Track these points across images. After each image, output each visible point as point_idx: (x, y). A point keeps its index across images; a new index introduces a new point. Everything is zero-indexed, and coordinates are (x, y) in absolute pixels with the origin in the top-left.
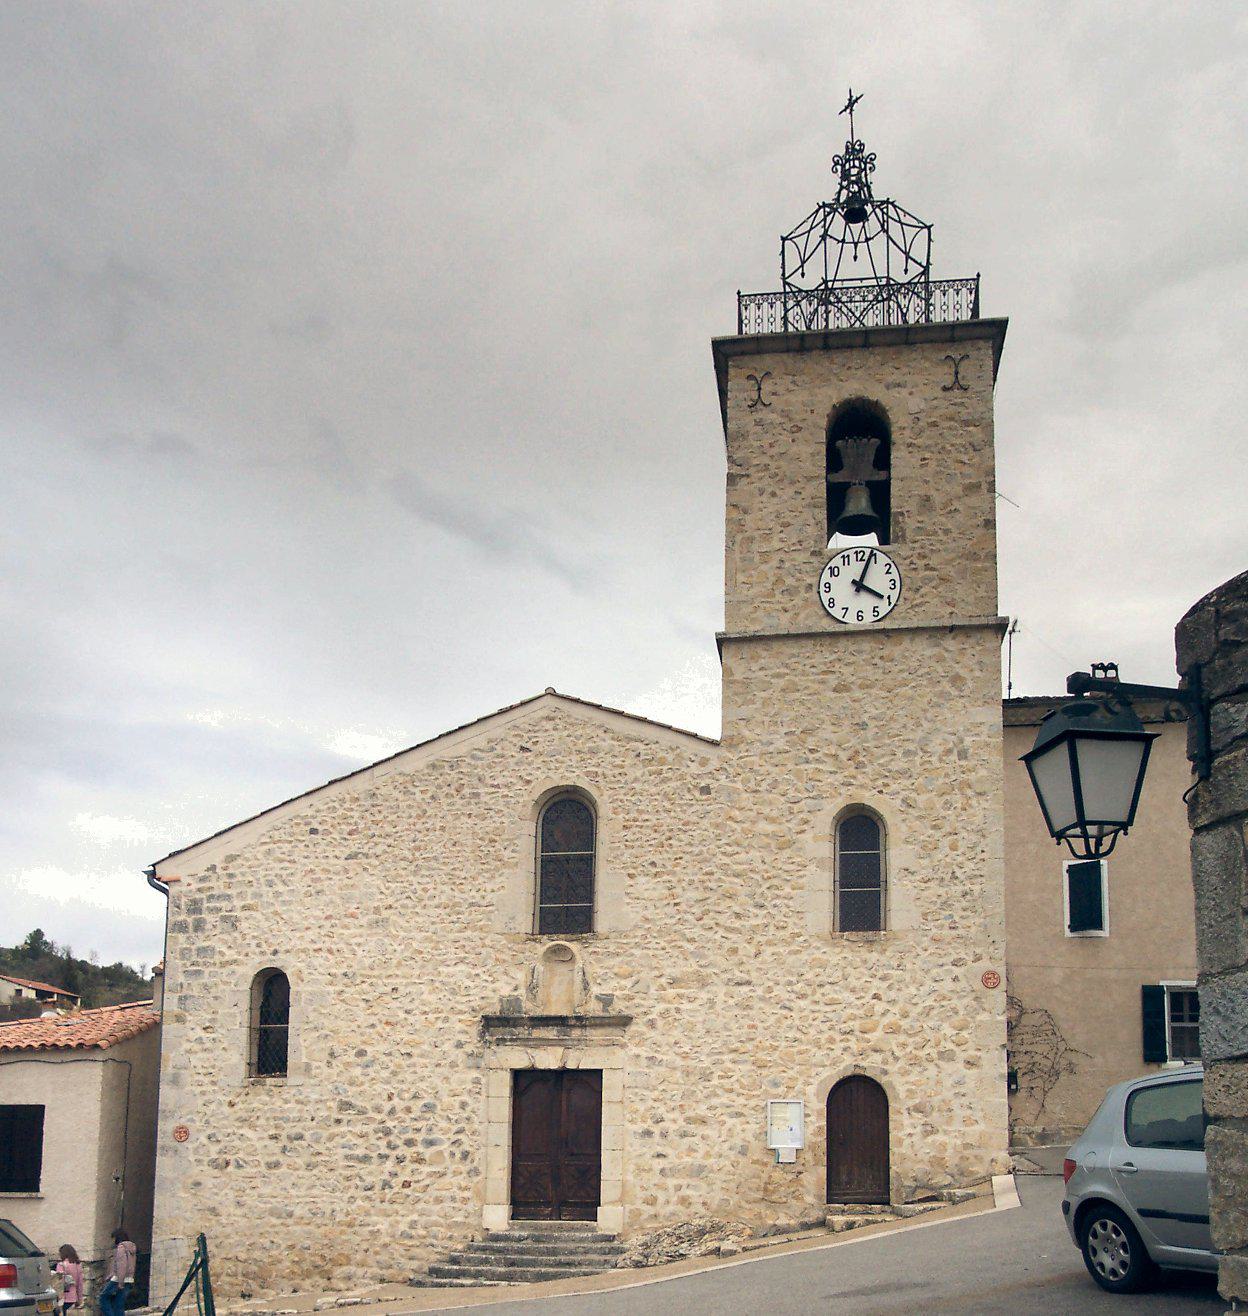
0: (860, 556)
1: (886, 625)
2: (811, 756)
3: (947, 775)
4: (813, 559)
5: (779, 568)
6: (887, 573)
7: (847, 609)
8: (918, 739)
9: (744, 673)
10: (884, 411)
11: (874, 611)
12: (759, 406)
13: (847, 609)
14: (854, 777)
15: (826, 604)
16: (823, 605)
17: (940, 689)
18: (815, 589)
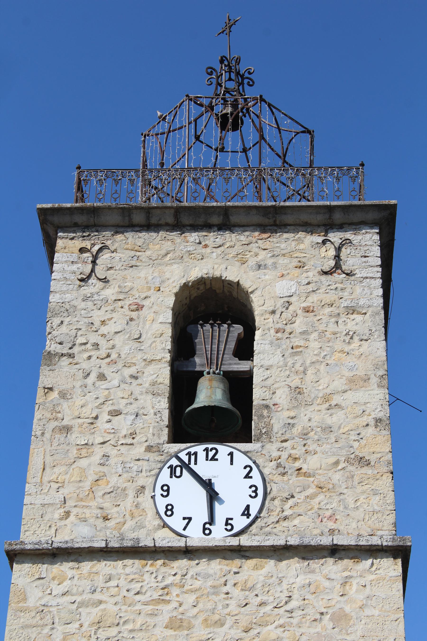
0: (211, 454)
6: (247, 476)
7: (190, 519)
9: (40, 598)
10: (247, 294)
11: (227, 524)
12: (93, 280)
13: (190, 519)
16: (158, 513)
17: (319, 629)
18: (148, 493)
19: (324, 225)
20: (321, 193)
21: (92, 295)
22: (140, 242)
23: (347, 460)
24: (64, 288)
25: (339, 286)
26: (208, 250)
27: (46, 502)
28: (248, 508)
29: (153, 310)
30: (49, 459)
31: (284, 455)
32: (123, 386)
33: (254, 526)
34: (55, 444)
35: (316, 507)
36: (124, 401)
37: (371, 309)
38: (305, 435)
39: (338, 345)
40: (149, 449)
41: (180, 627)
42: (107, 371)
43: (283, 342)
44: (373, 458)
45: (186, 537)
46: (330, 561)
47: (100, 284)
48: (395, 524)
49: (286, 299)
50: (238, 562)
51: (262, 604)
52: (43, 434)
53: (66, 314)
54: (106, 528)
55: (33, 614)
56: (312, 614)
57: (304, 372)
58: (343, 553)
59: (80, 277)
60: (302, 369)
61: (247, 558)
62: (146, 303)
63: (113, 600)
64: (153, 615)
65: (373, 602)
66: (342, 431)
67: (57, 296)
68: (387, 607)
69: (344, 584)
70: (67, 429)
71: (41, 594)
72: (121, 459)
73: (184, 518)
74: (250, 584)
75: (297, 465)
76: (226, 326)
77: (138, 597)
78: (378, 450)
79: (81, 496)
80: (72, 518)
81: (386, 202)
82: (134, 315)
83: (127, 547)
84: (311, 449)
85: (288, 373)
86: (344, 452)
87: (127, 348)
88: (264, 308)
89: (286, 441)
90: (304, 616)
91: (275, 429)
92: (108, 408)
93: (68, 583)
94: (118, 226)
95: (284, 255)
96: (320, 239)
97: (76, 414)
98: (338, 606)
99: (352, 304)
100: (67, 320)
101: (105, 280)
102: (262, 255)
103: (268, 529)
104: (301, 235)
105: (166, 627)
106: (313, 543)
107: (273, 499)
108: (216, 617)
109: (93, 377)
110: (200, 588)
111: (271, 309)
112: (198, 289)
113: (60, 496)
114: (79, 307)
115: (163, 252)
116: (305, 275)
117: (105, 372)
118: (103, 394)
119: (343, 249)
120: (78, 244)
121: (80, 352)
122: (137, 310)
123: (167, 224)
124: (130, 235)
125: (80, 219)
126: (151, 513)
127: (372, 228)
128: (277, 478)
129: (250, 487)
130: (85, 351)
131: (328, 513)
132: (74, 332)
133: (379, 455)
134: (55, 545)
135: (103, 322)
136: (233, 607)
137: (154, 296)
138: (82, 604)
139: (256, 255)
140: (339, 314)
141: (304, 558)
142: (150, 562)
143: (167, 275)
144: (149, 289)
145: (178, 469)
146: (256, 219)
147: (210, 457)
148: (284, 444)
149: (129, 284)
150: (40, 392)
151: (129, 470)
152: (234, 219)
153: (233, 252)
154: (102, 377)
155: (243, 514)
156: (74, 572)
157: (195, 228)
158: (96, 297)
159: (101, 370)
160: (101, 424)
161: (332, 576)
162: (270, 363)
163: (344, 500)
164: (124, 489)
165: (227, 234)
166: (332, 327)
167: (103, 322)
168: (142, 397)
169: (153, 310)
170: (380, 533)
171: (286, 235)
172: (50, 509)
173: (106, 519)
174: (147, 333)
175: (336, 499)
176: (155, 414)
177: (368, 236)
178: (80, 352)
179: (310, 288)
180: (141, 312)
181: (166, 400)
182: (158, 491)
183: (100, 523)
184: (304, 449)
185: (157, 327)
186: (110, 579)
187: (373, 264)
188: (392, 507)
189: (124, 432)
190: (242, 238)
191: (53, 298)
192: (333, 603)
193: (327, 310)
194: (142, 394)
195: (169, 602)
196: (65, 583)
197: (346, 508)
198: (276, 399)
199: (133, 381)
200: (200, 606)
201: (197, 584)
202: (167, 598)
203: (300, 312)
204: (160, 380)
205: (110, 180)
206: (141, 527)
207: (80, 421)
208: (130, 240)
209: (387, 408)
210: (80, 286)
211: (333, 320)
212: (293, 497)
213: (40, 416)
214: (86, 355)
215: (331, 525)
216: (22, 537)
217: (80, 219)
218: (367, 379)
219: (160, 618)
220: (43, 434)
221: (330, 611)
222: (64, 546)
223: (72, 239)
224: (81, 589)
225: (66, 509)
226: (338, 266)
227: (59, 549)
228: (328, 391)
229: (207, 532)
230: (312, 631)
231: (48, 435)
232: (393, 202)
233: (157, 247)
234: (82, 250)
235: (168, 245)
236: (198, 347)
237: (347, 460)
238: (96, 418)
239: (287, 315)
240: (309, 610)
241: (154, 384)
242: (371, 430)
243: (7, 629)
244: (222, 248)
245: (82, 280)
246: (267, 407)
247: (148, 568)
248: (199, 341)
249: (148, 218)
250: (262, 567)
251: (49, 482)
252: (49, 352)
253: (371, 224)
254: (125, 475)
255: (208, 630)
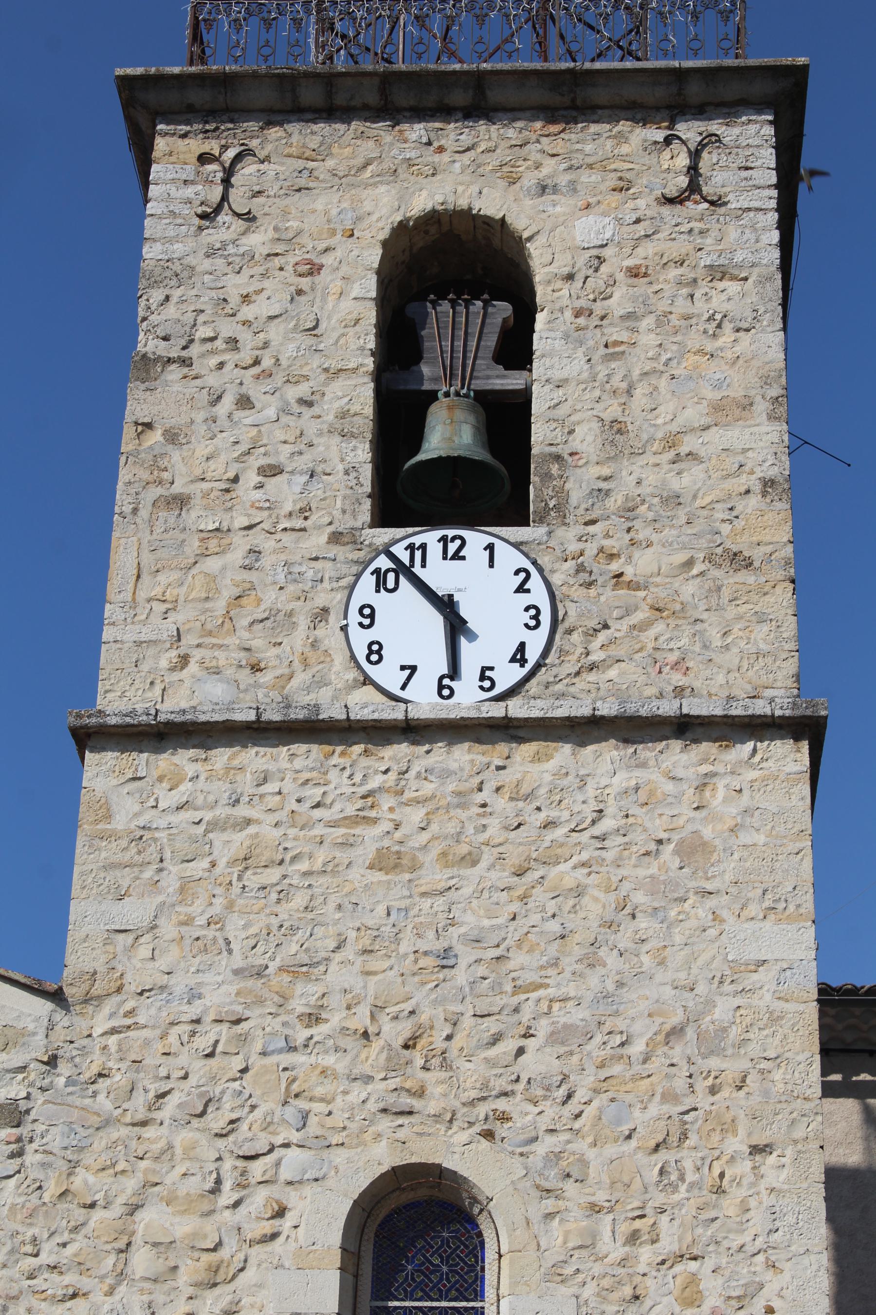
0: (452, 547)
1: (517, 708)
2: (301, 1035)
3: (669, 1097)
4: (335, 550)
5: (247, 568)
6: (521, 589)
7: (413, 669)
8: (590, 996)
9: (136, 815)
11: (482, 678)
12: (224, 217)
13: (413, 669)
14: (420, 1093)
15: (361, 654)
16: (353, 657)
17: (653, 870)
18: (335, 621)
19: (669, 107)
20: (663, 45)
21: (224, 247)
22: (313, 142)
23: (709, 558)
24: (171, 233)
25: (697, 225)
26: (446, 157)
27: (143, 637)
28: (522, 647)
29: (341, 274)
30: (147, 559)
31: (591, 549)
32: (284, 419)
33: (534, 682)
34: (158, 529)
35: (650, 645)
36: (288, 449)
37: (756, 271)
38: (629, 511)
39: (694, 340)
40: (336, 538)
41: (396, 866)
42: (255, 391)
43: (589, 334)
44: (757, 554)
45: (406, 702)
46: (676, 745)
47: (239, 225)
48: (798, 677)
49: (595, 252)
50: (503, 748)
51: (549, 825)
52: (135, 511)
53: (174, 282)
54: (257, 685)
55: (124, 843)
56: (641, 841)
57: (629, 392)
58: (700, 730)
59: (199, 210)
60: (624, 385)
61: (521, 740)
62: (328, 260)
63: (272, 818)
64: (345, 845)
65: (756, 821)
66: (699, 503)
67: (158, 247)
68: (780, 829)
69: (701, 787)
70: (181, 502)
71: (137, 808)
72: (283, 557)
73: (403, 668)
74: (525, 789)
75: (615, 567)
76: (479, 304)
77: (317, 813)
78: (768, 538)
79: (209, 626)
80: (193, 667)
81: (788, 61)
82: (305, 283)
83: (296, 721)
84: (641, 536)
85: (597, 393)
86: (703, 543)
87: (292, 346)
88: (552, 269)
89: (593, 522)
90: (626, 846)
91: (574, 500)
92: (257, 461)
93: (185, 787)
94: (271, 111)
95: (590, 166)
96: (659, 135)
97: (198, 472)
98: (690, 828)
99: (721, 261)
100: (176, 294)
101: (248, 217)
102: (549, 166)
103: (559, 687)
104: (624, 126)
105: (371, 867)
106: (643, 712)
107: (569, 632)
108: (464, 849)
109: (228, 402)
110: (433, 797)
111: (566, 270)
112: (426, 232)
113: (169, 627)
114: (199, 269)
115: (359, 161)
116: (631, 204)
117: (251, 393)
118: (247, 435)
119: (705, 155)
120: (196, 145)
121: (202, 356)
122: (310, 274)
123: (366, 107)
124: (294, 128)
125: (198, 97)
126: (340, 658)
127: (760, 112)
128: (577, 593)
129: (527, 609)
130: (213, 352)
131: (673, 658)
132: (189, 317)
133: (769, 549)
134: (162, 718)
135: (246, 298)
136: (494, 831)
137: (343, 248)
138: (214, 826)
139: (538, 166)
140: (695, 280)
141: (626, 741)
142: (339, 749)
143: (368, 206)
144: (333, 232)
145: (391, 576)
146: (537, 95)
147: (450, 554)
148: (591, 529)
149: (294, 224)
150: (129, 432)
151: (296, 578)
152: (495, 96)
153: (493, 161)
154: (245, 402)
155: (513, 660)
156: (199, 766)
157: (419, 114)
158: (231, 249)
159: (244, 390)
160: (246, 491)
161: (680, 773)
162: (564, 374)
163: (702, 633)
164: (290, 614)
165: (482, 126)
166: (682, 306)
167: (246, 298)
168: (322, 440)
169: (341, 274)
170: (769, 693)
171: (594, 128)
172: (151, 651)
173: (256, 668)
174: (329, 318)
175: (688, 630)
176: (347, 473)
177: (753, 128)
178: (202, 356)
179: (641, 229)
180: (317, 279)
181: (367, 446)
182: (354, 617)
183: (245, 677)
184: (628, 537)
185: (347, 306)
186: (265, 780)
187: (762, 182)
188: (792, 645)
189: (288, 507)
190: (511, 133)
191: (150, 252)
192: (681, 821)
193: (673, 273)
194: (320, 434)
195: (375, 821)
196: (182, 788)
197: (705, 647)
198: (576, 444)
199: (304, 409)
200: (434, 828)
201: (428, 788)
202: (373, 814)
203: (620, 276)
204: (355, 408)
205: (255, 20)
206: (321, 682)
207: (205, 486)
208: (295, 139)
209: (785, 458)
210: (200, 229)
211: (685, 291)
212: (606, 626)
213: (127, 478)
214: (213, 361)
215: (678, 679)
216: (101, 703)
217: (198, 97)
218: (747, 405)
219: (359, 851)
220: (135, 511)
221: (676, 837)
222: (179, 719)
223: (184, 136)
224: (211, 798)
225: (182, 651)
226: (694, 187)
227: (170, 725)
228: (674, 428)
229: (446, 692)
230: (641, 872)
231: (144, 513)
232: (802, 60)
233: (347, 151)
234: (204, 159)
235: (368, 148)
236: (427, 344)
237: (709, 558)
238: (236, 480)
239: (596, 282)
240: (637, 836)
241: (343, 415)
242: (754, 501)
243: (77, 870)
244: (471, 154)
245: (203, 216)
246: (558, 458)
247: (335, 760)
248: (431, 331)
249: (330, 94)
250: (549, 757)
251: (149, 600)
252: (144, 356)
253: (757, 105)
254: (291, 588)
255: (449, 872)
